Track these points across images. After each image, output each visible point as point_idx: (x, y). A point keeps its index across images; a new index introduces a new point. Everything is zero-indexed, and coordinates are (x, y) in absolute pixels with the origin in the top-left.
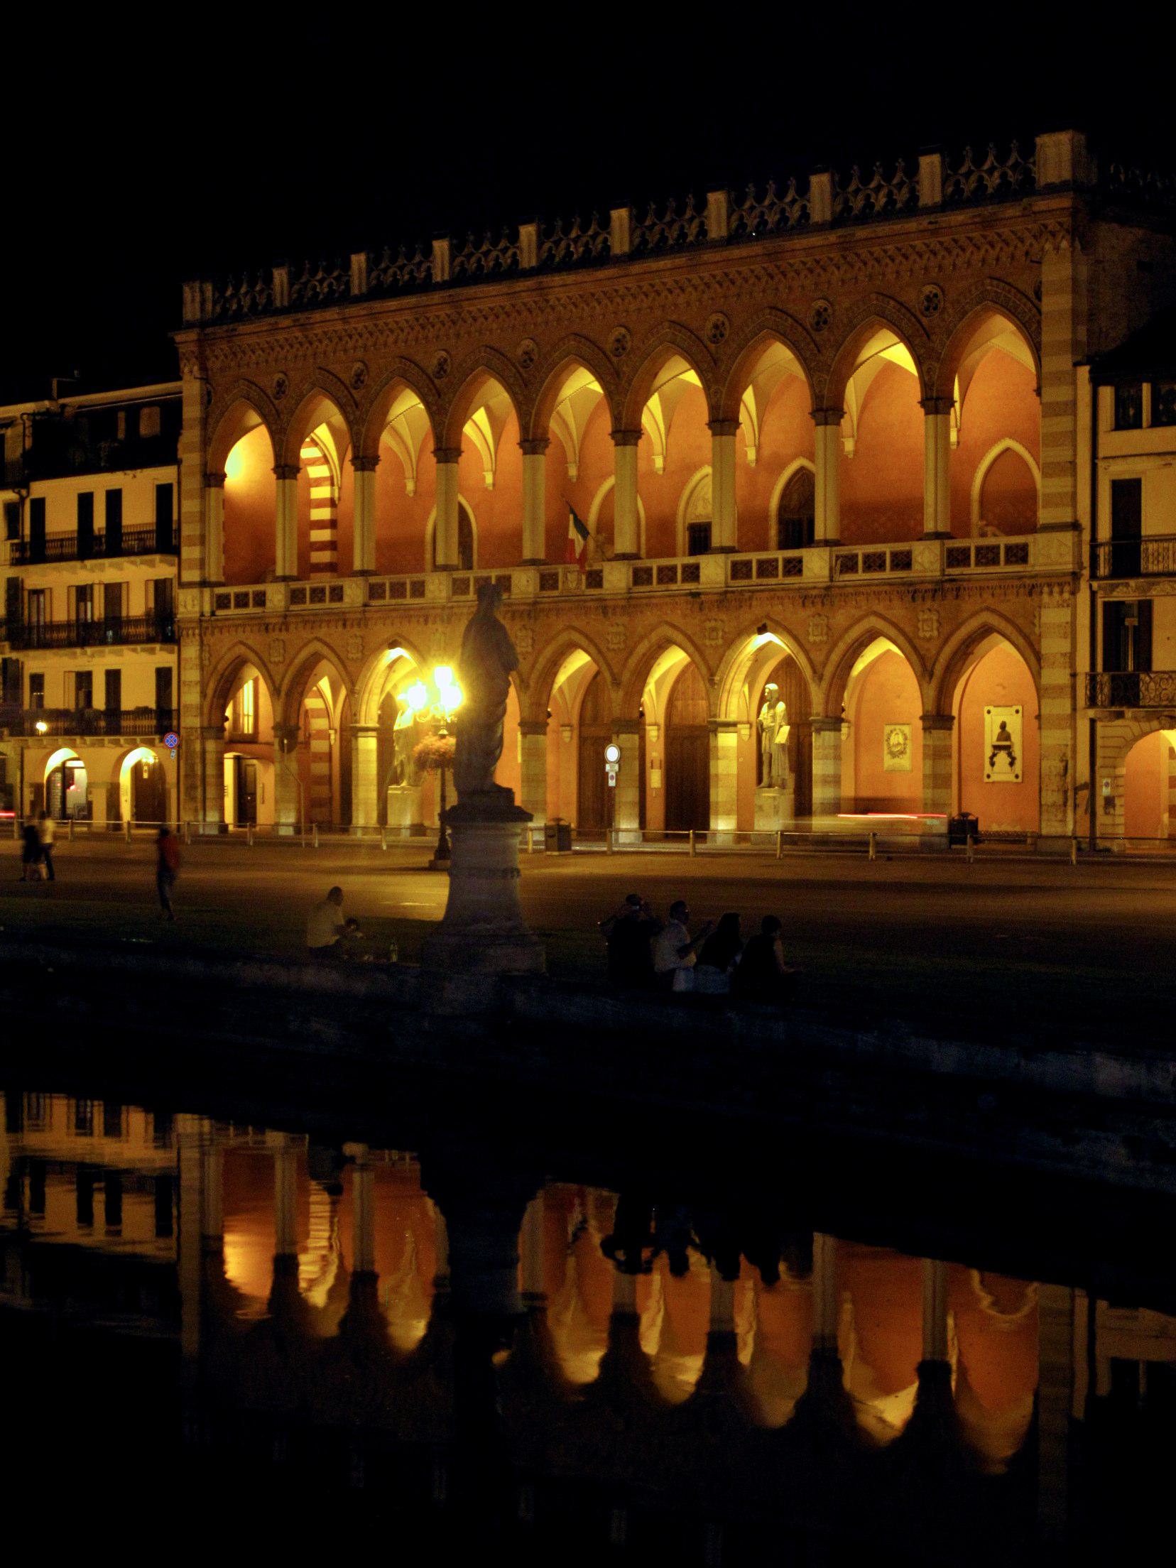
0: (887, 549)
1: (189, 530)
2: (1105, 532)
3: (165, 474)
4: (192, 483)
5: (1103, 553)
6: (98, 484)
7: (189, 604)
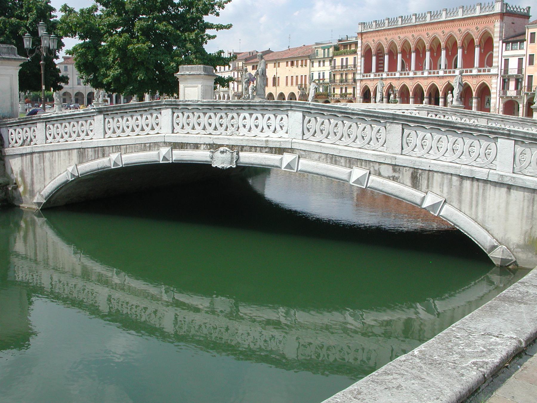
0: (469, 70)
1: (359, 64)
2: (503, 68)
3: (356, 56)
4: (359, 57)
5: (503, 71)
6: (344, 58)
7: (358, 77)
